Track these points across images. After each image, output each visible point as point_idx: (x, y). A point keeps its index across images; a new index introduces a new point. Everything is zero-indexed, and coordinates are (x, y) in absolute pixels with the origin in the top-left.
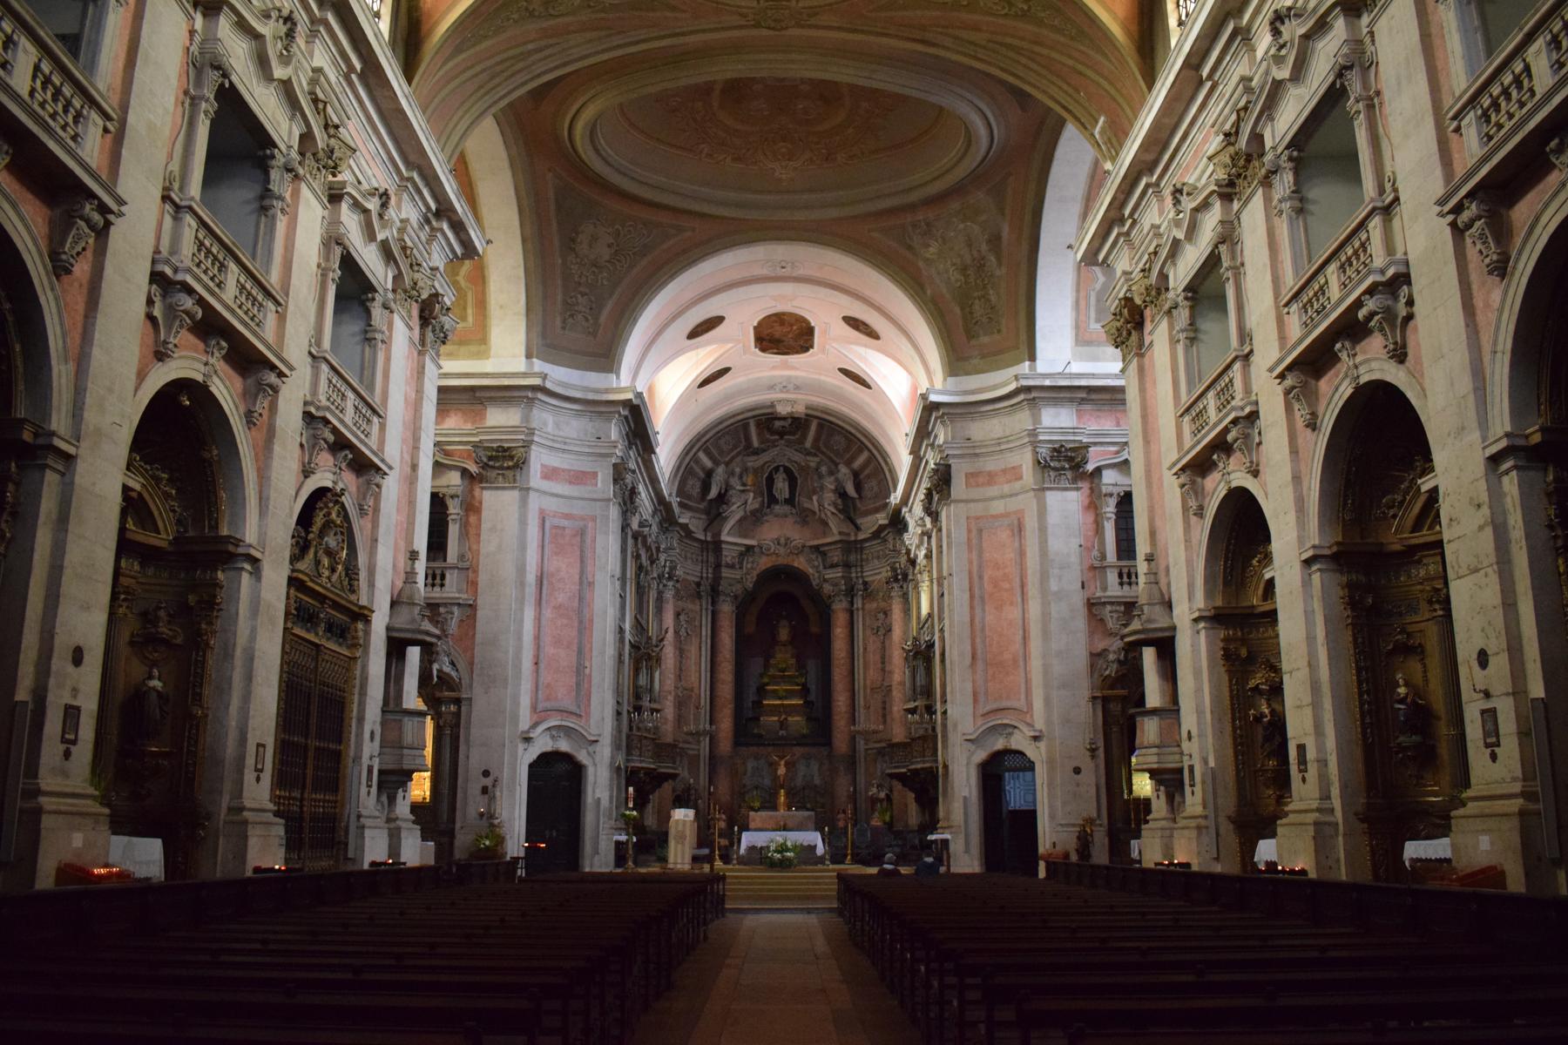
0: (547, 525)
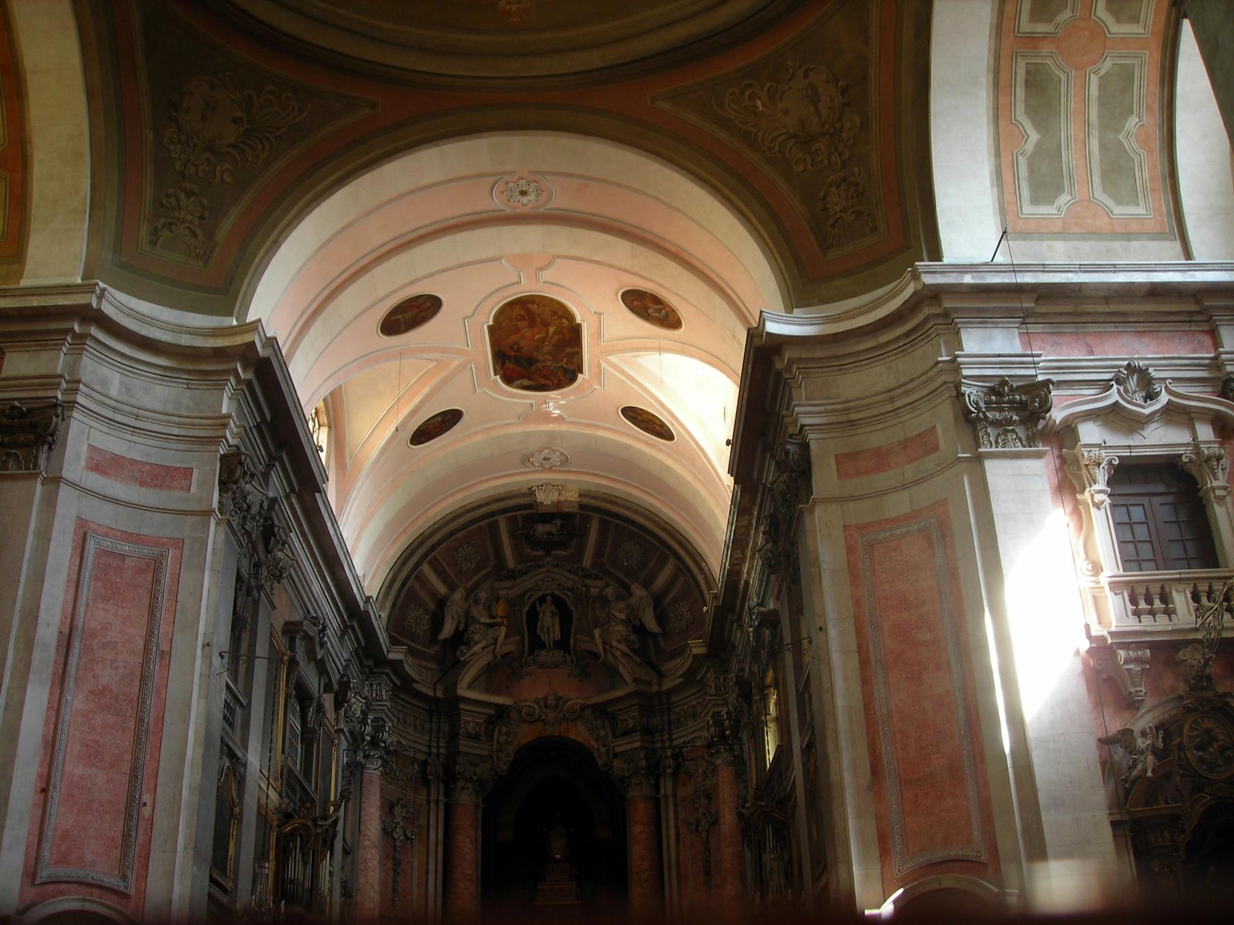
0: (91, 546)
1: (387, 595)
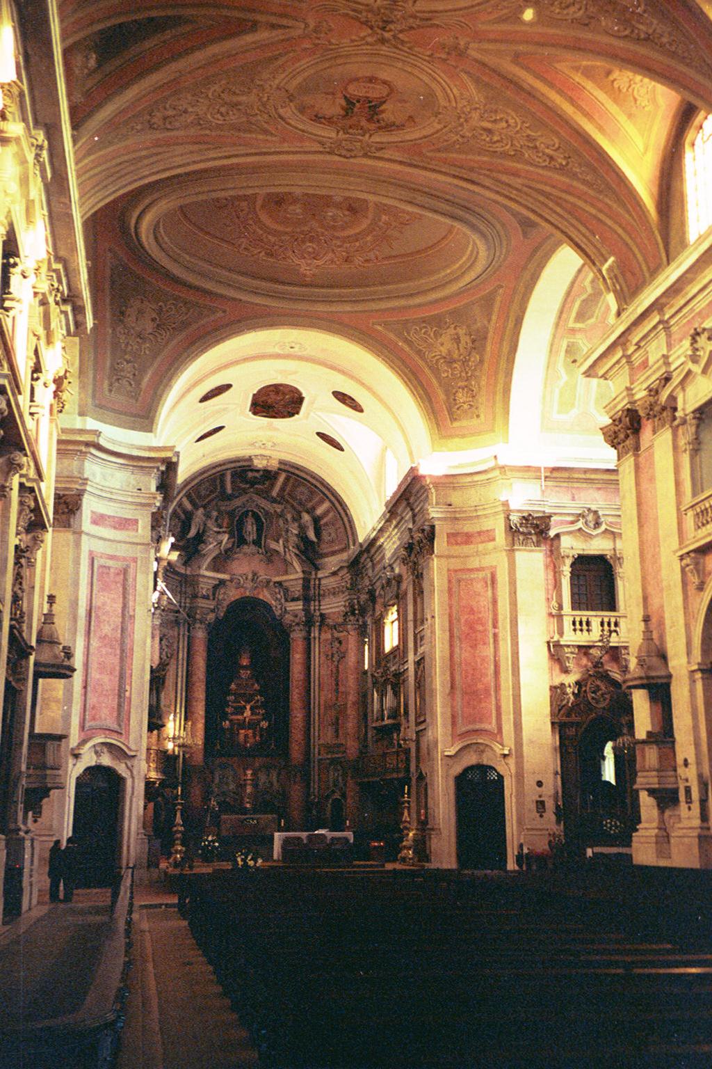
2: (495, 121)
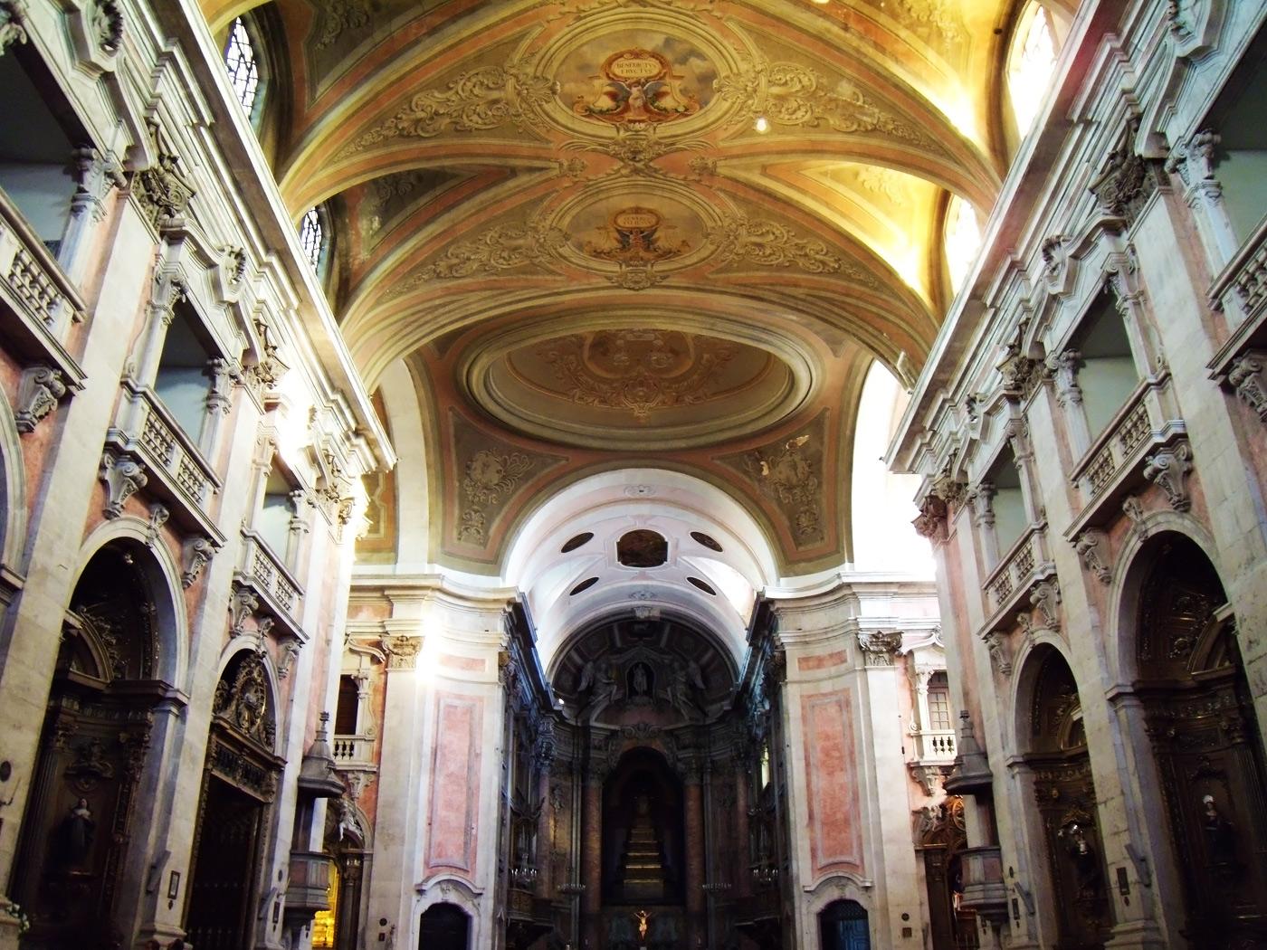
1: (552, 670)
2: (762, 234)
